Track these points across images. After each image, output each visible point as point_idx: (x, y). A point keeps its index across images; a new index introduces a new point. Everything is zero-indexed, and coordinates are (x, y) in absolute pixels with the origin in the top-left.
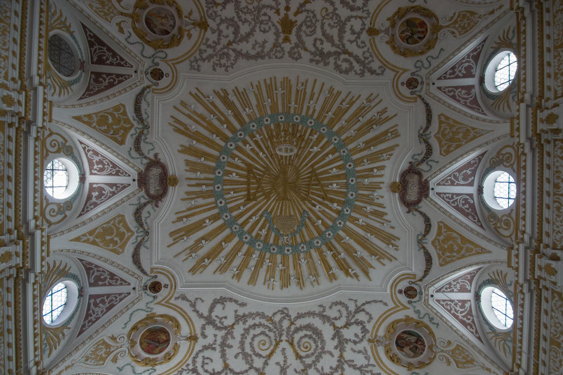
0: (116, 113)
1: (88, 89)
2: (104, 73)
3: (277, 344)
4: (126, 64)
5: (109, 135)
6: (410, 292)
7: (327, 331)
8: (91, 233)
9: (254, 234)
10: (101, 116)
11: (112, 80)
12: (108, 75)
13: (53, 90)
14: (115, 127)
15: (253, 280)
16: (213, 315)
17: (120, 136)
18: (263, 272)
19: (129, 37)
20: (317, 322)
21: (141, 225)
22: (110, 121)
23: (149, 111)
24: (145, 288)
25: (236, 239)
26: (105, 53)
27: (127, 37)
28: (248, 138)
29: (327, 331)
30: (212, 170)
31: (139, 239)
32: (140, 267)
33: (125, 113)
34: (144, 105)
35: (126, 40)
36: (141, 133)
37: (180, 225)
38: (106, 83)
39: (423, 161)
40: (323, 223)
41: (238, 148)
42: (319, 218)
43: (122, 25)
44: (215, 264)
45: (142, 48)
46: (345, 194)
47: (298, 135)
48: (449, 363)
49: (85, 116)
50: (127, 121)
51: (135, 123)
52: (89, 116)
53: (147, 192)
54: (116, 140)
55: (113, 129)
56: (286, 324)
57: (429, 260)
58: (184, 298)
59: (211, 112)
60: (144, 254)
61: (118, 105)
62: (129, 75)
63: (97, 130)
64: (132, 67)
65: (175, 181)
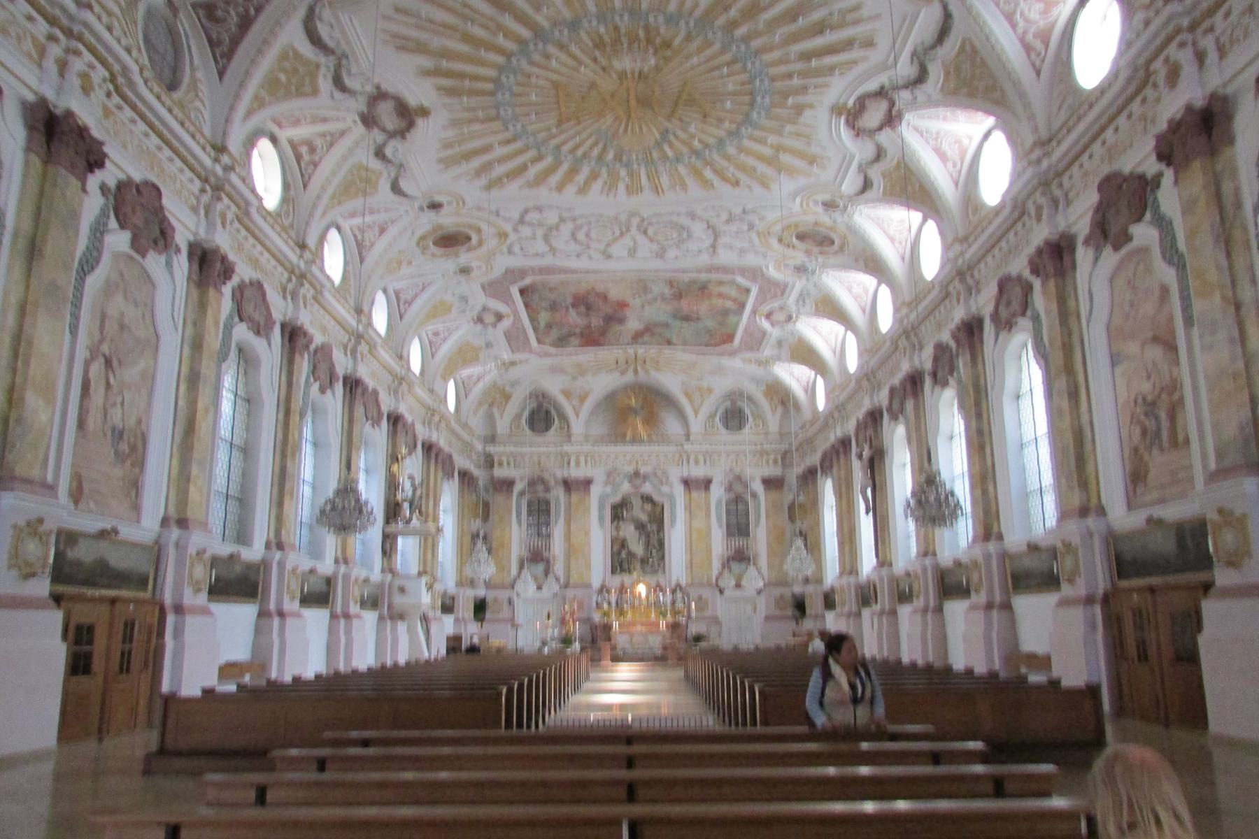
0: (287, 65)
1: (213, 44)
3: (622, 234)
6: (829, 205)
7: (698, 229)
8: (333, 197)
9: (579, 153)
15: (583, 190)
16: (528, 218)
18: (597, 186)
20: (685, 221)
21: (389, 161)
22: (283, 77)
23: (337, 34)
24: (421, 209)
25: (549, 160)
28: (551, 49)
29: (698, 229)
30: (492, 94)
31: (393, 174)
32: (405, 195)
33: (297, 55)
34: (323, 31)
36: (338, 66)
37: (450, 152)
38: (234, 19)
39: (906, 87)
40: (700, 141)
41: (533, 63)
42: (692, 136)
44: (520, 181)
46: (747, 115)
47: (658, 40)
48: (857, 260)
50: (306, 62)
51: (322, 59)
53: (384, 130)
56: (635, 221)
57: (867, 185)
58: (479, 209)
59: (465, 18)
60: (403, 184)
65: (424, 112)
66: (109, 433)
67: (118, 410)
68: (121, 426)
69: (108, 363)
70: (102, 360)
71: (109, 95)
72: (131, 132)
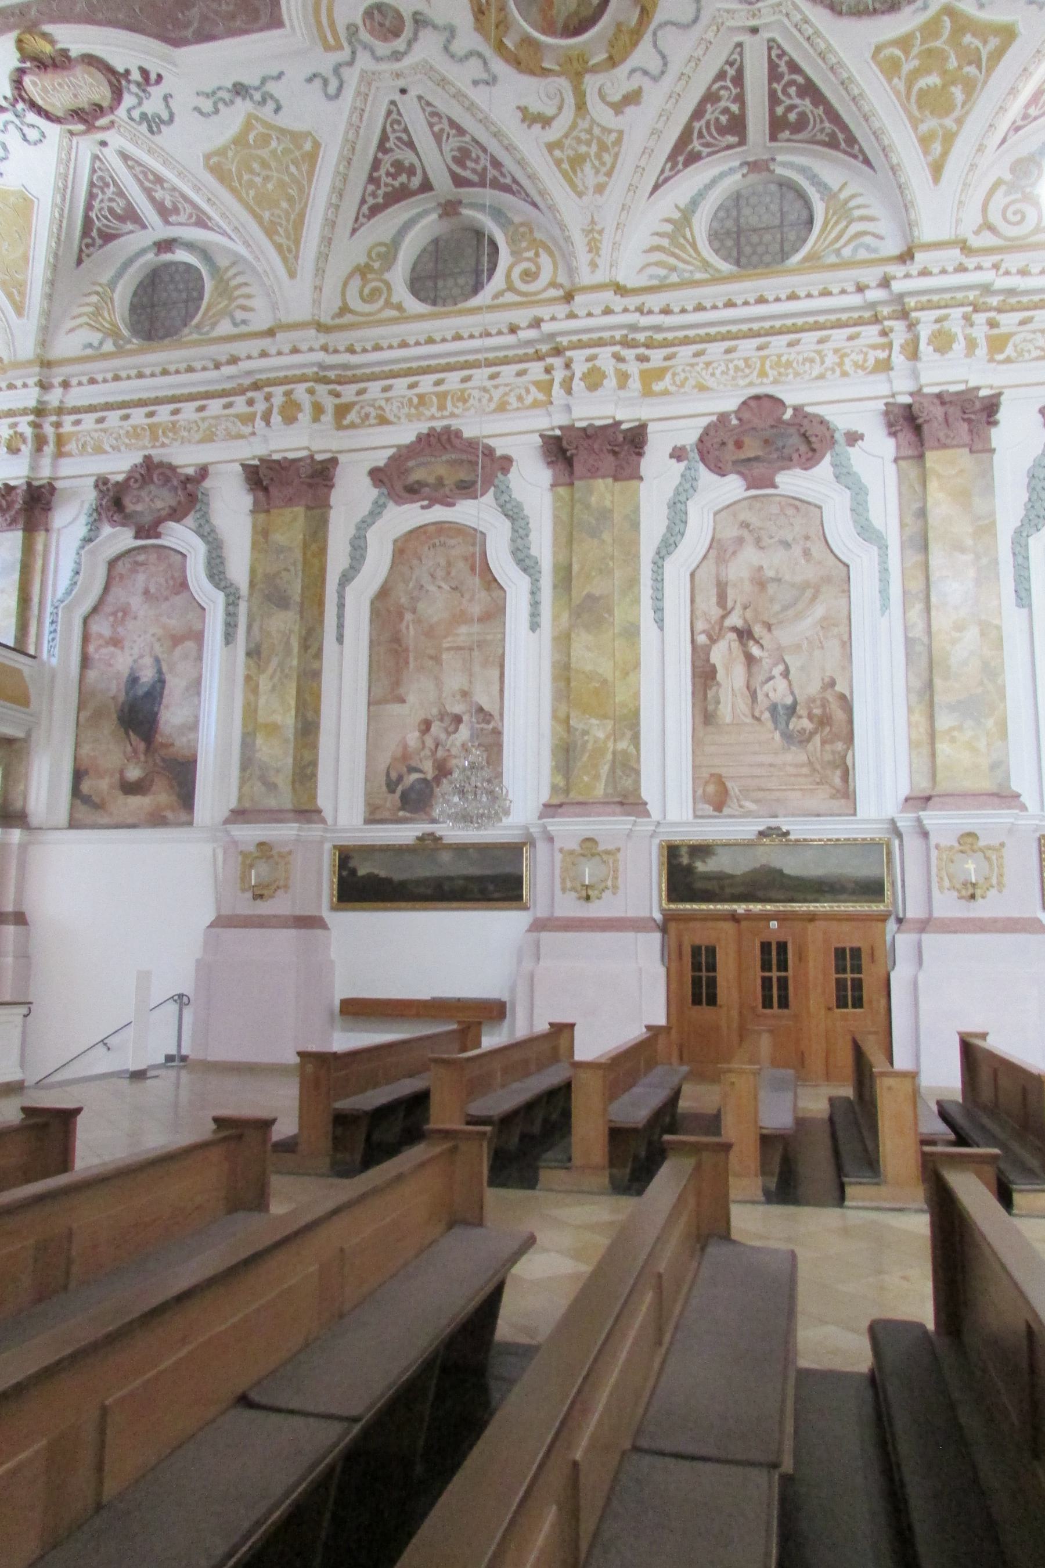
0: (907, 67)
2: (772, 112)
4: (731, 64)
5: (981, 77)
10: (920, 107)
11: (792, 90)
12: (774, 99)
13: (868, 239)
14: (953, 63)
17: (985, 42)
19: (646, 73)
22: (933, 80)
26: (708, 123)
27: (646, 79)
33: (904, 43)
35: (655, 79)
38: (805, 104)
43: (617, 98)
45: (669, 28)
49: (926, 153)
50: (931, 29)
52: (925, 141)
54: (998, 55)
55: (960, 68)
61: (879, 64)
62: (770, 49)
63: (967, 113)
64: (740, 45)
66: (767, 715)
67: (781, 684)
68: (789, 701)
69: (744, 634)
70: (733, 636)
71: (642, 359)
72: (708, 364)
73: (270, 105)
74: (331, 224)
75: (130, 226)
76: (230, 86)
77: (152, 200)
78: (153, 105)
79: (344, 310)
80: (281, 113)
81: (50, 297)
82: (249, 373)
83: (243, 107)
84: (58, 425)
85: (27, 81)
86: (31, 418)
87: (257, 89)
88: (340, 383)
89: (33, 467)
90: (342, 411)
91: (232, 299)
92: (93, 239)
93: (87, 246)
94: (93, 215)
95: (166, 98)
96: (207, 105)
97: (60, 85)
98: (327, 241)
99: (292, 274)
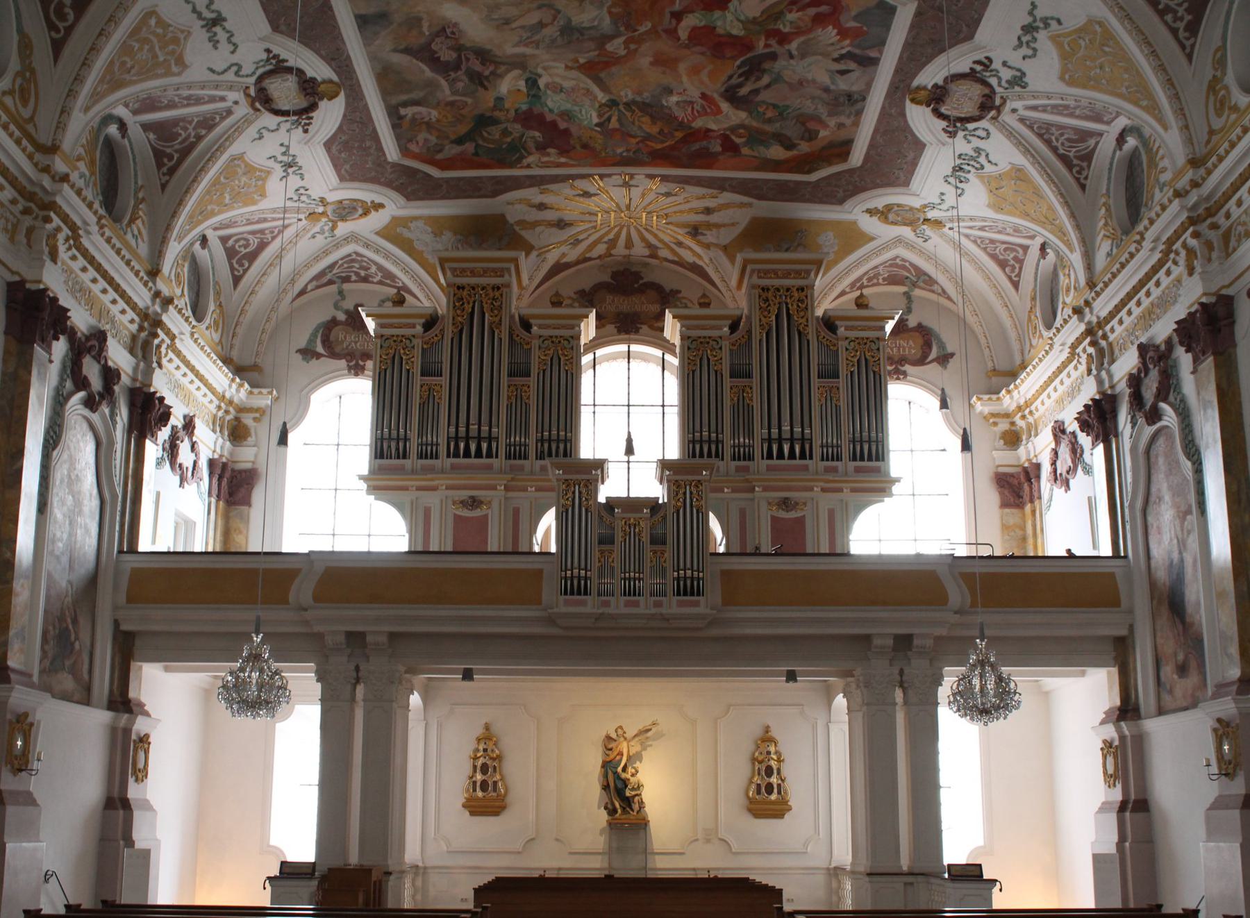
73: (1054, 24)
74: (1161, 68)
75: (1092, 142)
76: (1020, 32)
77: (1078, 117)
78: (1006, 74)
79: (1212, 132)
80: (1062, 20)
81: (1078, 227)
82: (1156, 240)
83: (1042, 35)
84: (1105, 337)
85: (943, 110)
86: (1088, 340)
87: (1035, 21)
88: (1213, 215)
89: (1100, 382)
90: (1226, 237)
91: (1157, 166)
92: (1078, 165)
93: (1079, 172)
94: (1061, 151)
95: (1005, 64)
96: (1025, 51)
97: (957, 100)
98: (1169, 83)
99: (1166, 128)
